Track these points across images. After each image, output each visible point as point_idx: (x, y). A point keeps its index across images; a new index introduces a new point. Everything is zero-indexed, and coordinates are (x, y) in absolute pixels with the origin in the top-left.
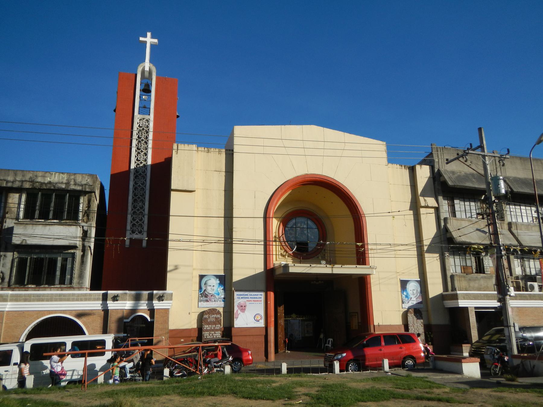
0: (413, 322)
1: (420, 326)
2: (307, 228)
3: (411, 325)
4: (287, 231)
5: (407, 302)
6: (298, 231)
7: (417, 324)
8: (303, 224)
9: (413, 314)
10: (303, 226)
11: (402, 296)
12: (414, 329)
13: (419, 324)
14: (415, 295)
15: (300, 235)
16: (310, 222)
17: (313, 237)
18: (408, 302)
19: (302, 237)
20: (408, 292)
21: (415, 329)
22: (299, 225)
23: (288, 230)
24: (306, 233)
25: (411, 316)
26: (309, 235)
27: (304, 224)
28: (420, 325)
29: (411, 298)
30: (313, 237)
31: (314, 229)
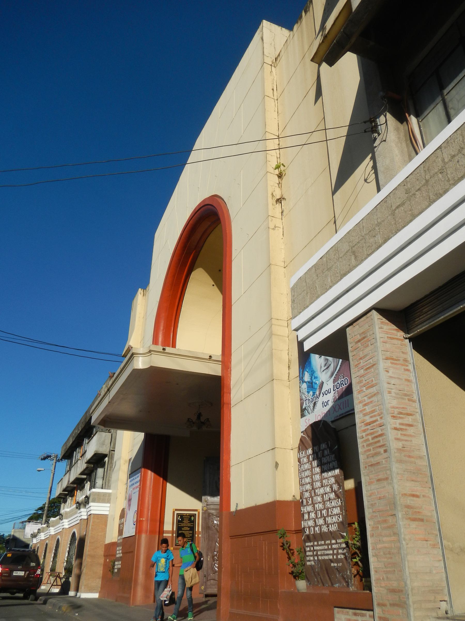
0: (313, 481)
1: (332, 496)
3: (306, 499)
5: (312, 405)
7: (322, 491)
9: (310, 451)
11: (300, 391)
12: (313, 515)
13: (328, 489)
14: (332, 365)
18: (315, 404)
20: (314, 368)
21: (316, 513)
25: (305, 460)
28: (332, 491)
29: (322, 383)
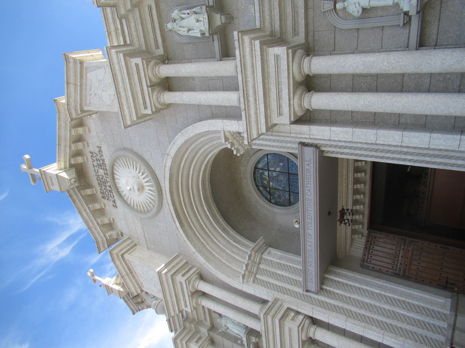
2: (268, 170)
4: (276, 201)
6: (274, 186)
8: (264, 176)
10: (266, 177)
15: (279, 184)
16: (260, 166)
17: (281, 164)
19: (282, 181)
22: (266, 182)
23: (275, 200)
24: (276, 173)
26: (278, 169)
27: (263, 174)
30: (281, 164)
31: (269, 161)
